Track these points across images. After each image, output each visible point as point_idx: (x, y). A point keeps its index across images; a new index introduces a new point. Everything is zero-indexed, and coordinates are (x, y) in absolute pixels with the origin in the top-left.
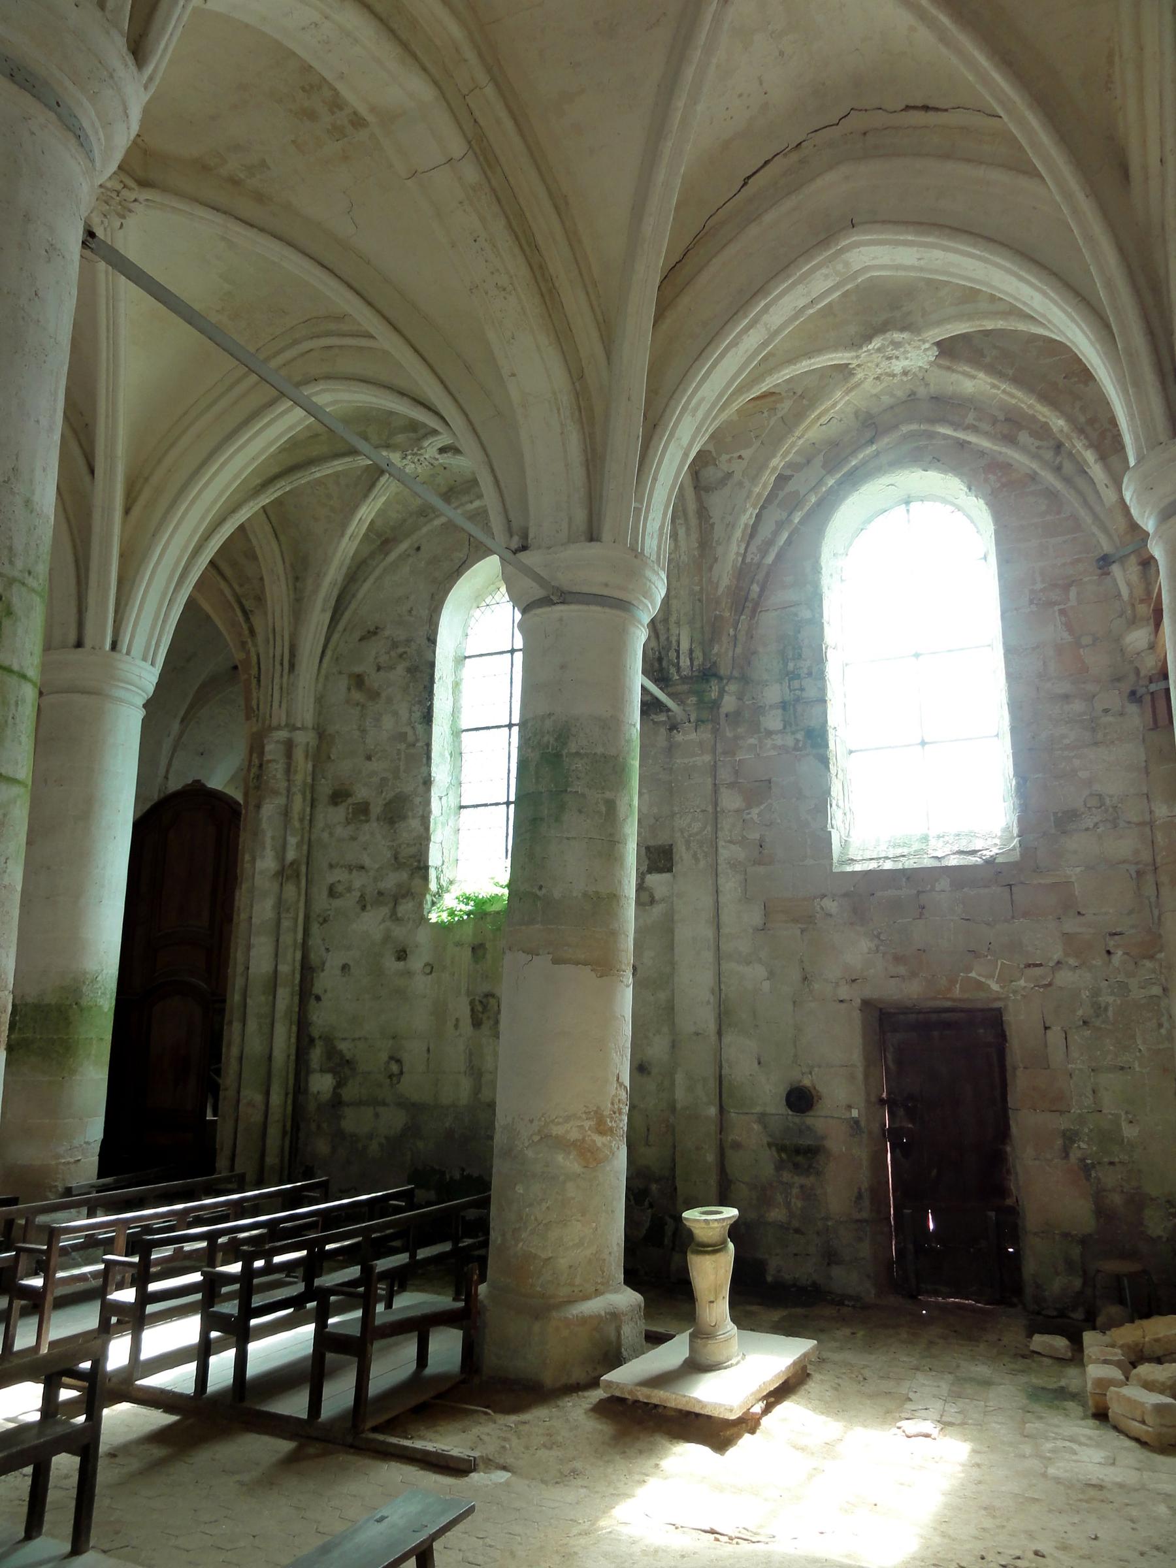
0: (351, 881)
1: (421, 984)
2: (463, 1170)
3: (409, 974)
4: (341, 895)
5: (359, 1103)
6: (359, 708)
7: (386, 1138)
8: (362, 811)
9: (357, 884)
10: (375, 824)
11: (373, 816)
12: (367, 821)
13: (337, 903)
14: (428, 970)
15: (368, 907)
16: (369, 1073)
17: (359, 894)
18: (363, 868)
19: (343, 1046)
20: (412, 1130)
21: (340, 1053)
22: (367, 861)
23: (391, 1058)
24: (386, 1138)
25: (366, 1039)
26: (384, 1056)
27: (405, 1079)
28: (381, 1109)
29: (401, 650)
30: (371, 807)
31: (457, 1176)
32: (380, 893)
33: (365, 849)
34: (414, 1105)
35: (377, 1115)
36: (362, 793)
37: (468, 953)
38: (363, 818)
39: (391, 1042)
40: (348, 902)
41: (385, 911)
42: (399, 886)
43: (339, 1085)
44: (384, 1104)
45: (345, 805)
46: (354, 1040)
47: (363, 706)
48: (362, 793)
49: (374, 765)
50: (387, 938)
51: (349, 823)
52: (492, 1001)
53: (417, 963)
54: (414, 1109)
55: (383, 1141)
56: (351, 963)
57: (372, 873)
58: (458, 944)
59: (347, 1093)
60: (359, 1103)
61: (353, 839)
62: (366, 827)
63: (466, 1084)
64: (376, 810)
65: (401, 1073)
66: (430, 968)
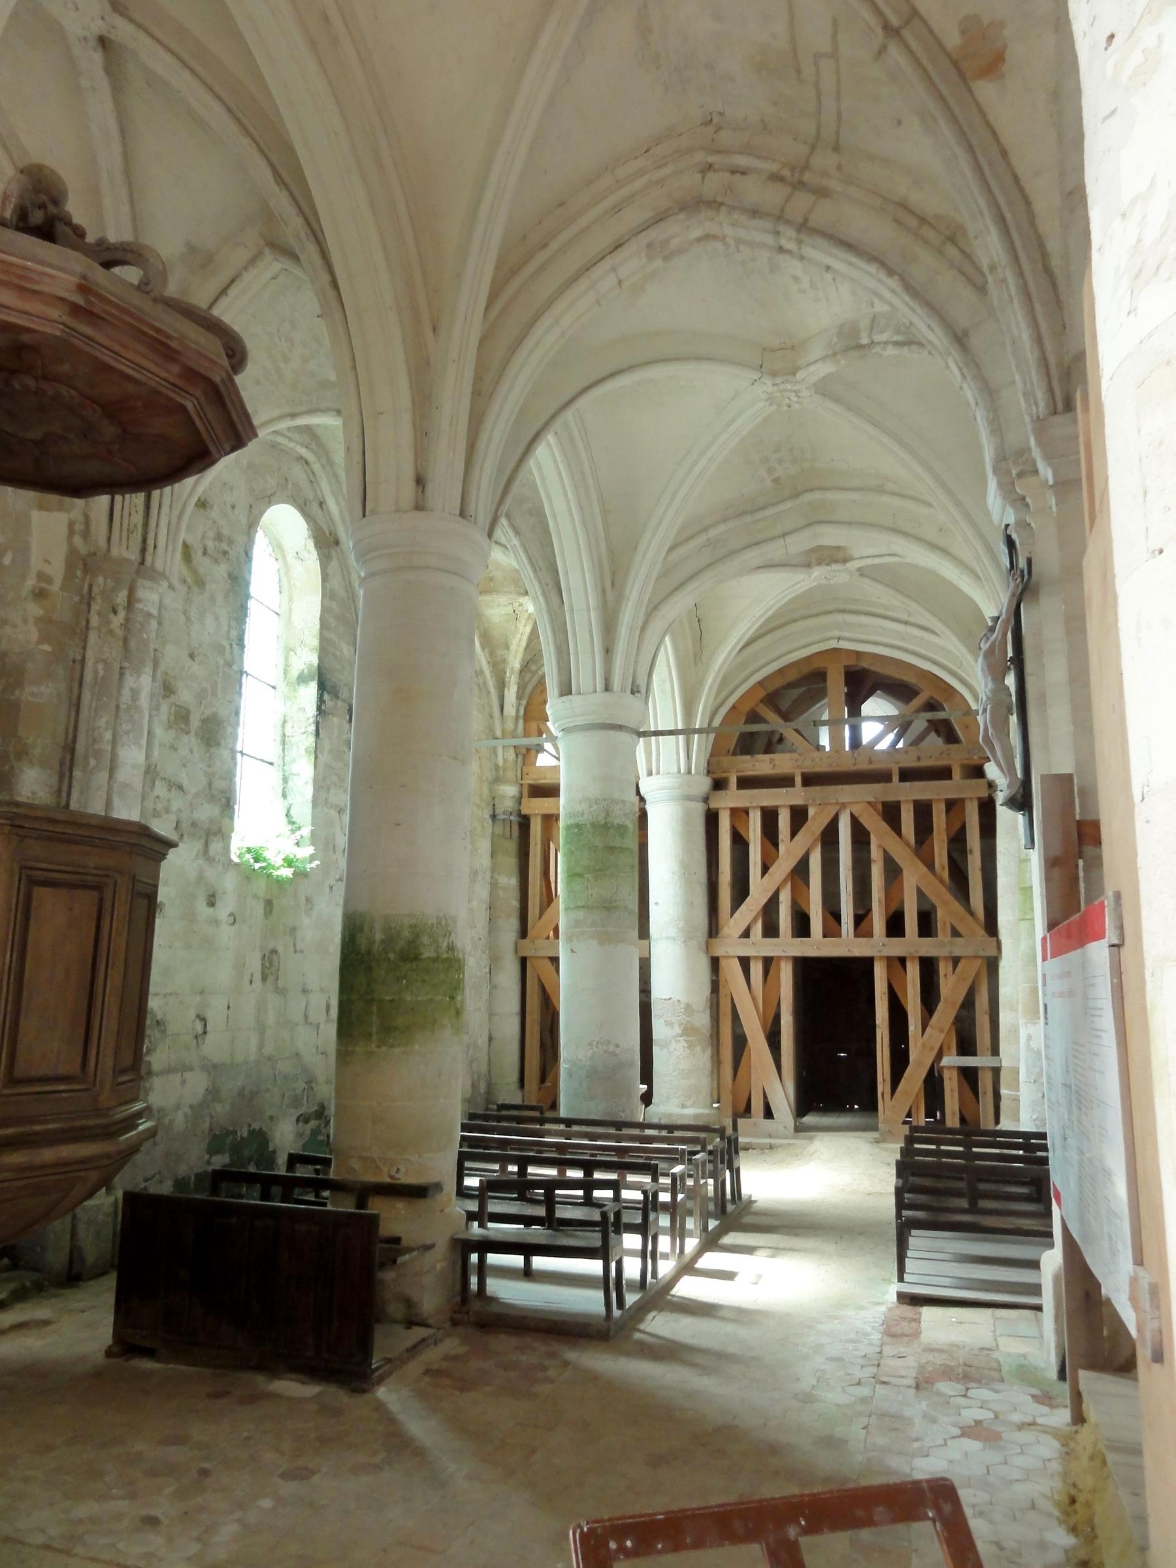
0: (169, 801)
1: (226, 933)
2: (250, 1125)
3: (216, 922)
5: (168, 1071)
7: (191, 1107)
8: (181, 717)
10: (193, 740)
11: (193, 733)
12: (188, 733)
14: (231, 920)
16: (178, 1034)
17: (173, 817)
18: (180, 787)
20: (213, 1094)
22: (185, 783)
23: (198, 1016)
24: (191, 1107)
25: (177, 994)
26: (192, 1014)
27: (210, 1038)
28: (187, 1075)
29: (224, 546)
30: (192, 717)
31: (245, 1134)
33: (184, 766)
34: (215, 1066)
35: (184, 1082)
37: (260, 909)
39: (199, 998)
41: (198, 845)
42: (212, 821)
44: (191, 1069)
47: (189, 588)
48: (185, 696)
49: (196, 668)
50: (200, 878)
51: (170, 727)
52: (275, 957)
53: (223, 911)
54: (213, 1069)
55: (188, 1110)
58: (255, 897)
60: (168, 1071)
61: (174, 748)
62: (185, 739)
63: (254, 1041)
64: (195, 722)
65: (205, 1033)
66: (234, 919)
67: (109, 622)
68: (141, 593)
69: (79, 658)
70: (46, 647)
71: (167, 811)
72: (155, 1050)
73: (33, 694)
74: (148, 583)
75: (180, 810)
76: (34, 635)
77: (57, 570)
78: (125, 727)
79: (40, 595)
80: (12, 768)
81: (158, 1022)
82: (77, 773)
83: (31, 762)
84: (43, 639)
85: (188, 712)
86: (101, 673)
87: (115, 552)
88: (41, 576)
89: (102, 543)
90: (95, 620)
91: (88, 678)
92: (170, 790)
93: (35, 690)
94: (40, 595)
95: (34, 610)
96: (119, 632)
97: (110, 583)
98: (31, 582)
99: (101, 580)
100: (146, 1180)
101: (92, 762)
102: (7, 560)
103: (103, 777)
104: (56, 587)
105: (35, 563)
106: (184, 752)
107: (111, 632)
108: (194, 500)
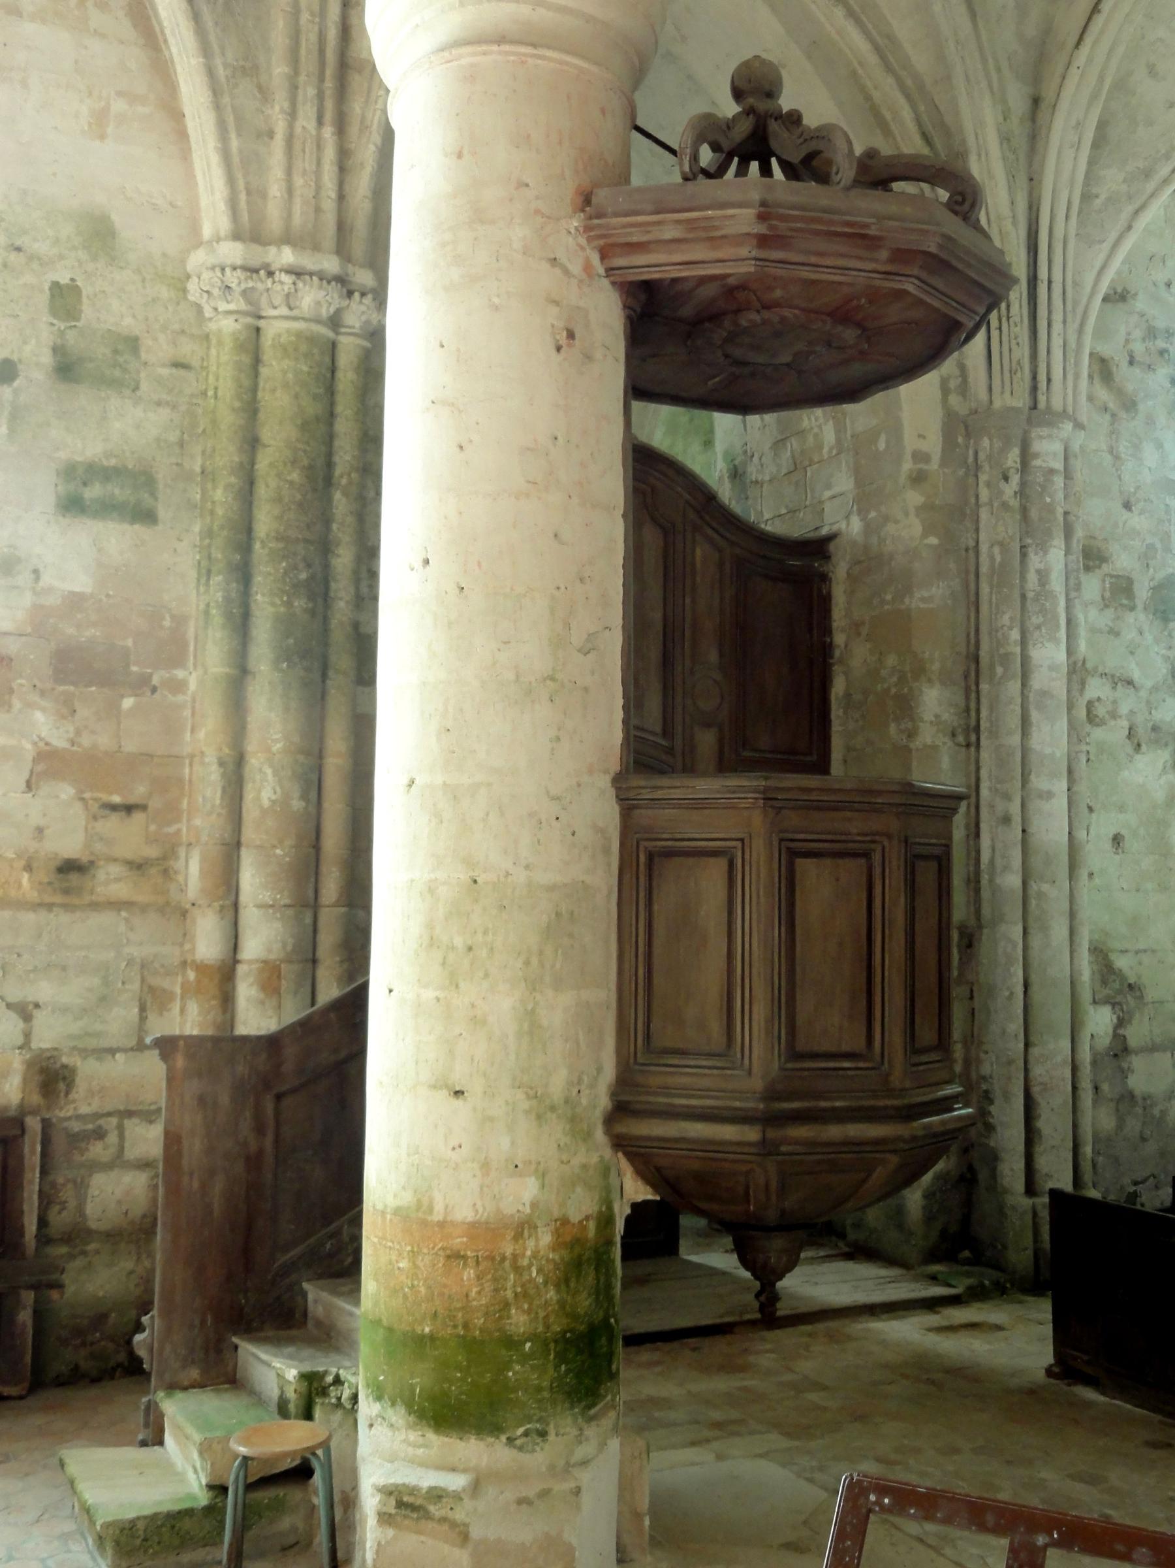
0: (1115, 702)
4: (1102, 723)
5: (1153, 1048)
6: (1108, 417)
9: (1124, 709)
10: (1142, 617)
11: (1140, 606)
12: (1132, 609)
13: (1098, 734)
15: (1144, 748)
16: (1162, 1002)
18: (1130, 683)
19: (1122, 963)
21: (1119, 974)
22: (1136, 675)
25: (1154, 951)
29: (1161, 344)
30: (1136, 586)
32: (1155, 729)
33: (1132, 653)
36: (1123, 561)
38: (1125, 602)
40: (1112, 734)
43: (1121, 1023)
45: (1098, 573)
46: (1137, 952)
47: (1113, 415)
48: (1123, 561)
49: (1136, 521)
51: (1106, 606)
56: (1123, 832)
57: (1143, 694)
59: (1135, 1034)
61: (1114, 633)
62: (1130, 618)
64: (1142, 592)
67: (1001, 493)
68: (1037, 446)
69: (972, 543)
70: (933, 540)
71: (1114, 715)
72: (1130, 1022)
73: (923, 599)
74: (1044, 431)
75: (1132, 712)
76: (917, 528)
77: (933, 444)
78: (1035, 620)
79: (918, 479)
80: (911, 689)
81: (1130, 985)
82: (984, 687)
83: (930, 680)
84: (927, 531)
85: (1130, 581)
86: (998, 558)
87: (997, 404)
88: (920, 457)
89: (983, 395)
90: (984, 494)
91: (984, 569)
92: (1114, 688)
93: (926, 594)
94: (918, 479)
95: (914, 498)
96: (1015, 503)
97: (998, 444)
98: (907, 466)
99: (986, 442)
100: (1136, 1183)
101: (999, 670)
102: (882, 445)
103: (1013, 687)
104: (934, 465)
105: (910, 443)
106: (1130, 635)
107: (1005, 506)
108: (1100, 296)
